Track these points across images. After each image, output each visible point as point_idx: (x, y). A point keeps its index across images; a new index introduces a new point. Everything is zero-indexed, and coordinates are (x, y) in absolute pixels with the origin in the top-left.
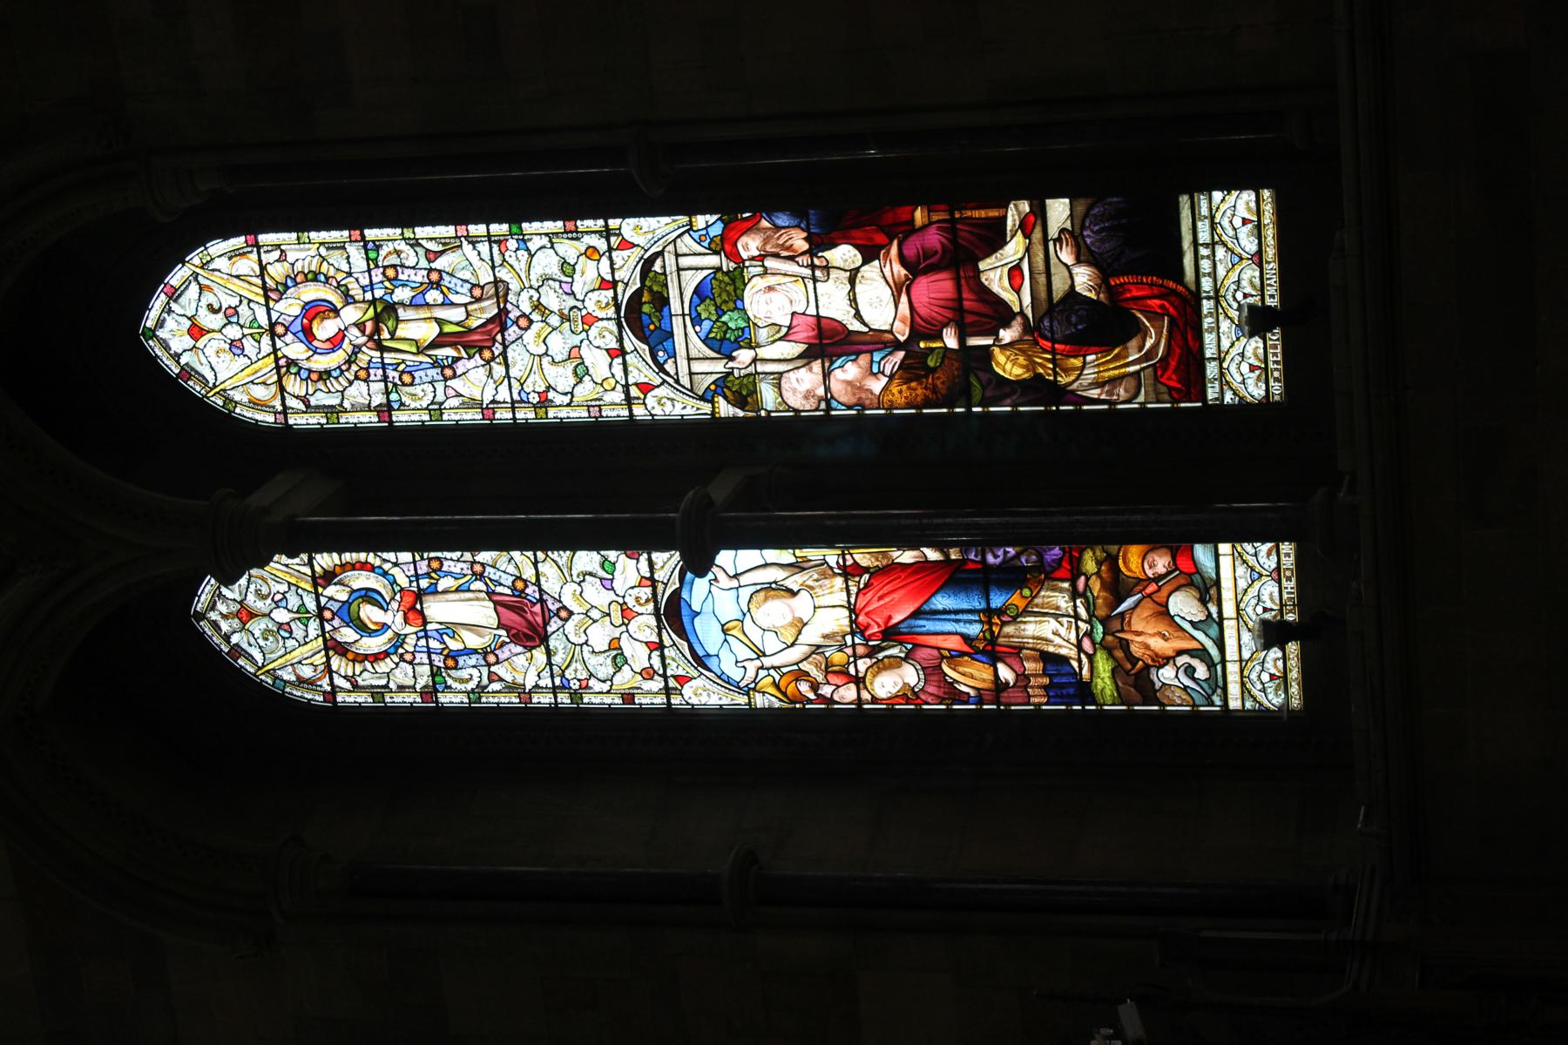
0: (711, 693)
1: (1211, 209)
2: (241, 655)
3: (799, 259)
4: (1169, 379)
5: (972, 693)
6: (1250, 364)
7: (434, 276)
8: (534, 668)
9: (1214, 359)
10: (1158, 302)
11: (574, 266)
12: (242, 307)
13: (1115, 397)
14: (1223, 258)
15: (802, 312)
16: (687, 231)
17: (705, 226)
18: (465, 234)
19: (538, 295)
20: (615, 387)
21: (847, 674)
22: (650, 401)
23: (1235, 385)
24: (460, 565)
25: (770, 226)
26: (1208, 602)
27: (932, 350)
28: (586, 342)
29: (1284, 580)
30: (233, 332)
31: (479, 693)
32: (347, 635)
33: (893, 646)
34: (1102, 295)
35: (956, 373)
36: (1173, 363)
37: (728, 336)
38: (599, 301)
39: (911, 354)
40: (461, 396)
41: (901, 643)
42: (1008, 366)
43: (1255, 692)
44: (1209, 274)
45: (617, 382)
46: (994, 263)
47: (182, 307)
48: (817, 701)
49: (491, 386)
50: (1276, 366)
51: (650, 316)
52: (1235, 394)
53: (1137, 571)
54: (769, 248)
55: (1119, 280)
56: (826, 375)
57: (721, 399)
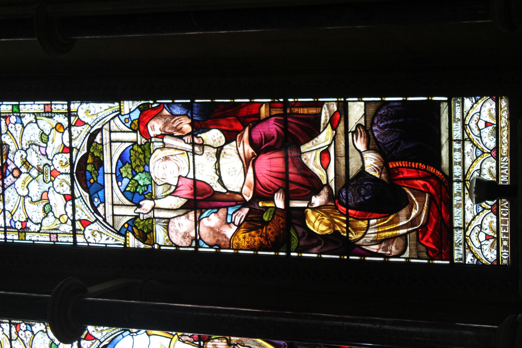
1: (463, 114)
3: (185, 138)
4: (427, 241)
6: (486, 235)
9: (460, 228)
10: (422, 182)
11: (48, 136)
13: (388, 252)
14: (470, 151)
15: (185, 176)
16: (117, 115)
17: (128, 112)
20: (67, 221)
23: (474, 249)
27: (267, 208)
28: (52, 189)
34: (383, 175)
36: (431, 230)
37: (138, 190)
38: (61, 161)
39: (253, 210)
42: (317, 224)
44: (459, 163)
45: (68, 218)
46: (311, 147)
50: (505, 237)
51: (91, 173)
52: (474, 256)
54: (167, 130)
55: (395, 164)
56: (197, 222)
57: (130, 235)
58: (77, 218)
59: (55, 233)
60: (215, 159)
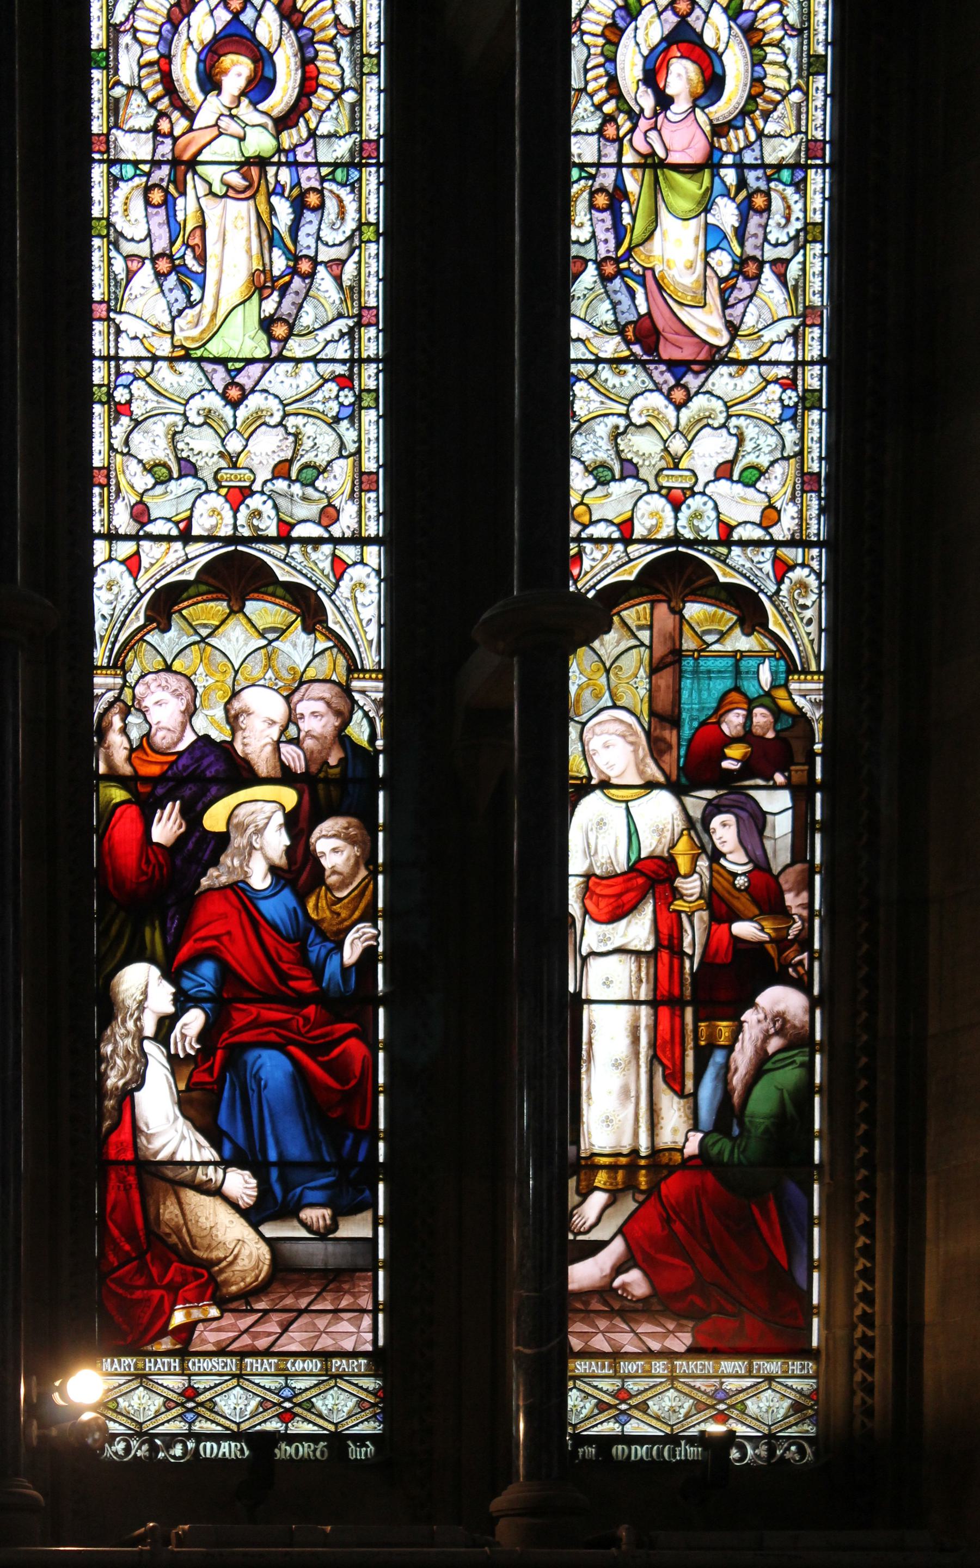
7: (305, 266)
38: (260, 514)
40: (128, 281)
58: (145, 545)
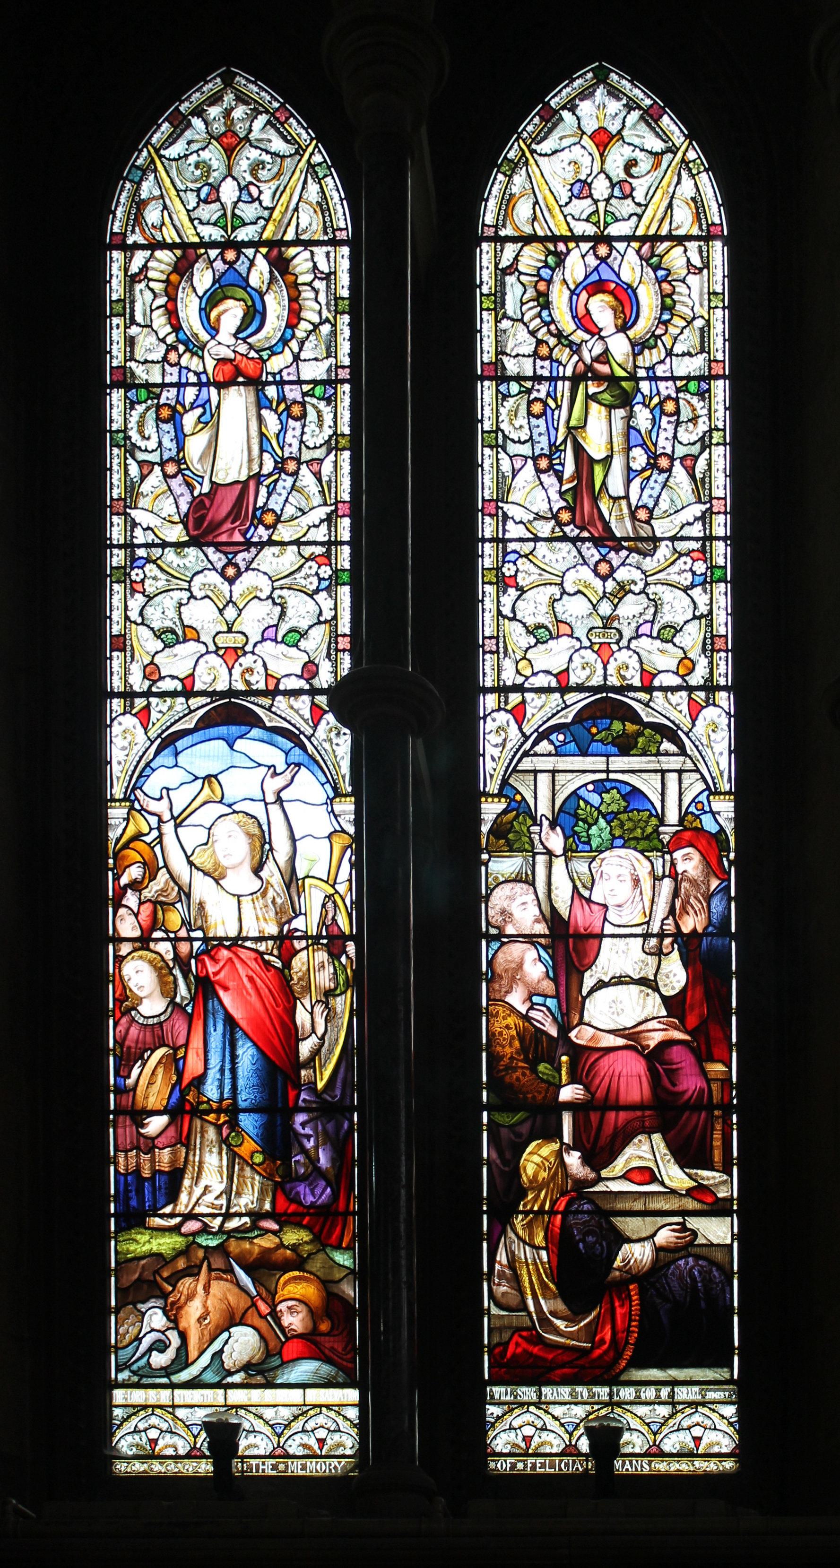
0: (126, 752)
1: (713, 1403)
2: (175, 128)
3: (670, 921)
4: (517, 1345)
5: (130, 1082)
6: (532, 1437)
8: (159, 524)
9: (540, 1397)
10: (608, 1337)
11: (671, 641)
12: (632, 205)
13: (497, 1280)
16: (708, 788)
17: (714, 809)
18: (715, 510)
19: (637, 591)
20: (521, 674)
21: (154, 926)
22: (503, 717)
23: (508, 1419)
24: (296, 444)
25: (713, 888)
26: (246, 1373)
27: (559, 1071)
29: (273, 1461)
30: (601, 188)
31: (125, 446)
32: (203, 279)
33: (189, 990)
34: (617, 1273)
35: (530, 1096)
36: (536, 1350)
37: (581, 823)
38: (627, 667)
40: (514, 476)
41: (193, 999)
42: (536, 1159)
43: (134, 1420)
44: (639, 1397)
45: (527, 678)
47: (634, 126)
48: (117, 887)
49: (527, 517)
50: (530, 1465)
51: (608, 729)
52: (498, 1418)
53: (285, 1292)
54: (685, 885)
56: (530, 939)
58: (529, 696)
59: (498, 647)
60: (636, 977)
